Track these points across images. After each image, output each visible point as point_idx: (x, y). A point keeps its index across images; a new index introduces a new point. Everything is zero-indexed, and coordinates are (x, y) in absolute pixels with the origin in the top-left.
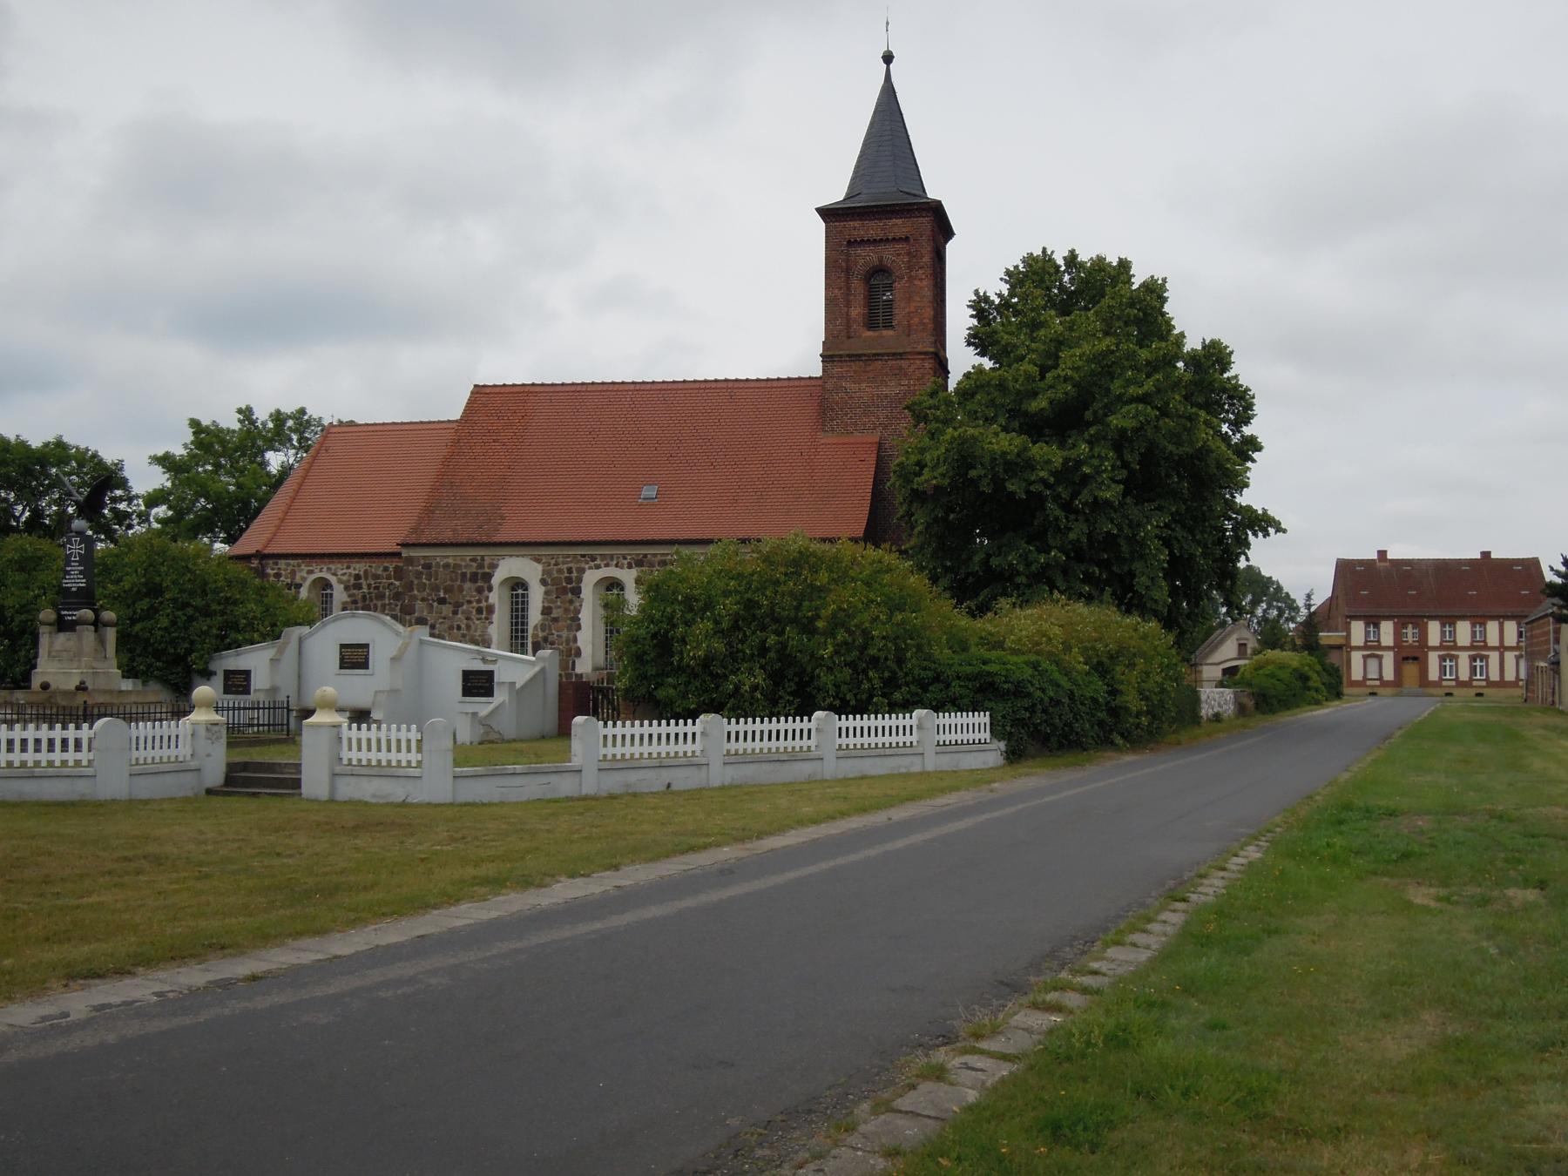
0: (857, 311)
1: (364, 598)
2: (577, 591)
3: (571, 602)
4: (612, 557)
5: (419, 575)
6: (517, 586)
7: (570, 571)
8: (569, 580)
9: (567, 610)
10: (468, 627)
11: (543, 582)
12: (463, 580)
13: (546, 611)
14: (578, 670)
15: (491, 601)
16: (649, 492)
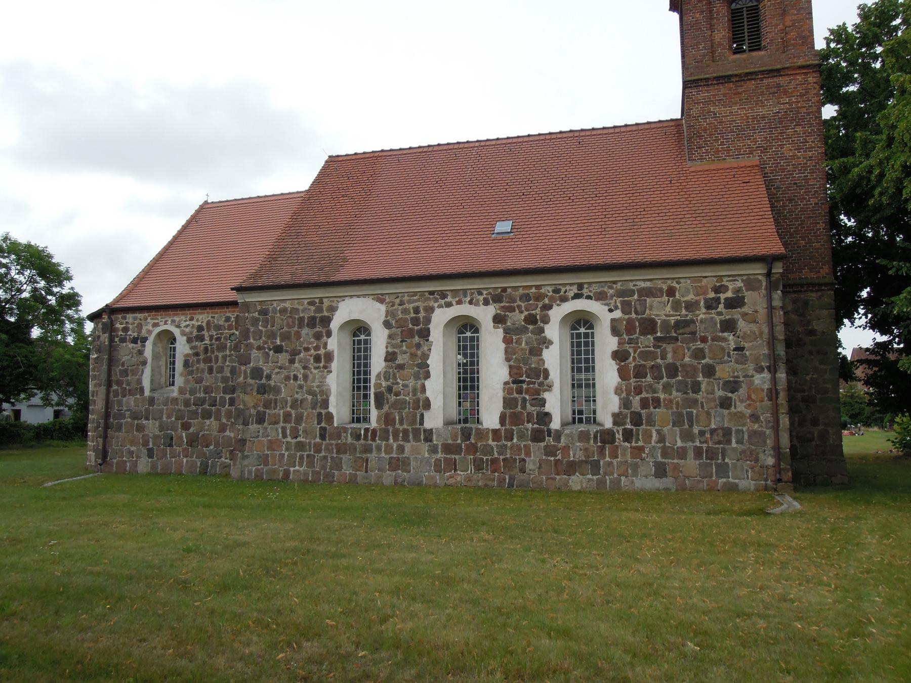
0: (722, 34)
1: (206, 350)
2: (425, 334)
3: (418, 346)
5: (255, 322)
6: (359, 329)
7: (417, 310)
8: (416, 321)
9: (413, 356)
10: (306, 377)
11: (387, 324)
12: (301, 326)
13: (390, 357)
14: (428, 425)
15: (329, 347)
16: (504, 227)
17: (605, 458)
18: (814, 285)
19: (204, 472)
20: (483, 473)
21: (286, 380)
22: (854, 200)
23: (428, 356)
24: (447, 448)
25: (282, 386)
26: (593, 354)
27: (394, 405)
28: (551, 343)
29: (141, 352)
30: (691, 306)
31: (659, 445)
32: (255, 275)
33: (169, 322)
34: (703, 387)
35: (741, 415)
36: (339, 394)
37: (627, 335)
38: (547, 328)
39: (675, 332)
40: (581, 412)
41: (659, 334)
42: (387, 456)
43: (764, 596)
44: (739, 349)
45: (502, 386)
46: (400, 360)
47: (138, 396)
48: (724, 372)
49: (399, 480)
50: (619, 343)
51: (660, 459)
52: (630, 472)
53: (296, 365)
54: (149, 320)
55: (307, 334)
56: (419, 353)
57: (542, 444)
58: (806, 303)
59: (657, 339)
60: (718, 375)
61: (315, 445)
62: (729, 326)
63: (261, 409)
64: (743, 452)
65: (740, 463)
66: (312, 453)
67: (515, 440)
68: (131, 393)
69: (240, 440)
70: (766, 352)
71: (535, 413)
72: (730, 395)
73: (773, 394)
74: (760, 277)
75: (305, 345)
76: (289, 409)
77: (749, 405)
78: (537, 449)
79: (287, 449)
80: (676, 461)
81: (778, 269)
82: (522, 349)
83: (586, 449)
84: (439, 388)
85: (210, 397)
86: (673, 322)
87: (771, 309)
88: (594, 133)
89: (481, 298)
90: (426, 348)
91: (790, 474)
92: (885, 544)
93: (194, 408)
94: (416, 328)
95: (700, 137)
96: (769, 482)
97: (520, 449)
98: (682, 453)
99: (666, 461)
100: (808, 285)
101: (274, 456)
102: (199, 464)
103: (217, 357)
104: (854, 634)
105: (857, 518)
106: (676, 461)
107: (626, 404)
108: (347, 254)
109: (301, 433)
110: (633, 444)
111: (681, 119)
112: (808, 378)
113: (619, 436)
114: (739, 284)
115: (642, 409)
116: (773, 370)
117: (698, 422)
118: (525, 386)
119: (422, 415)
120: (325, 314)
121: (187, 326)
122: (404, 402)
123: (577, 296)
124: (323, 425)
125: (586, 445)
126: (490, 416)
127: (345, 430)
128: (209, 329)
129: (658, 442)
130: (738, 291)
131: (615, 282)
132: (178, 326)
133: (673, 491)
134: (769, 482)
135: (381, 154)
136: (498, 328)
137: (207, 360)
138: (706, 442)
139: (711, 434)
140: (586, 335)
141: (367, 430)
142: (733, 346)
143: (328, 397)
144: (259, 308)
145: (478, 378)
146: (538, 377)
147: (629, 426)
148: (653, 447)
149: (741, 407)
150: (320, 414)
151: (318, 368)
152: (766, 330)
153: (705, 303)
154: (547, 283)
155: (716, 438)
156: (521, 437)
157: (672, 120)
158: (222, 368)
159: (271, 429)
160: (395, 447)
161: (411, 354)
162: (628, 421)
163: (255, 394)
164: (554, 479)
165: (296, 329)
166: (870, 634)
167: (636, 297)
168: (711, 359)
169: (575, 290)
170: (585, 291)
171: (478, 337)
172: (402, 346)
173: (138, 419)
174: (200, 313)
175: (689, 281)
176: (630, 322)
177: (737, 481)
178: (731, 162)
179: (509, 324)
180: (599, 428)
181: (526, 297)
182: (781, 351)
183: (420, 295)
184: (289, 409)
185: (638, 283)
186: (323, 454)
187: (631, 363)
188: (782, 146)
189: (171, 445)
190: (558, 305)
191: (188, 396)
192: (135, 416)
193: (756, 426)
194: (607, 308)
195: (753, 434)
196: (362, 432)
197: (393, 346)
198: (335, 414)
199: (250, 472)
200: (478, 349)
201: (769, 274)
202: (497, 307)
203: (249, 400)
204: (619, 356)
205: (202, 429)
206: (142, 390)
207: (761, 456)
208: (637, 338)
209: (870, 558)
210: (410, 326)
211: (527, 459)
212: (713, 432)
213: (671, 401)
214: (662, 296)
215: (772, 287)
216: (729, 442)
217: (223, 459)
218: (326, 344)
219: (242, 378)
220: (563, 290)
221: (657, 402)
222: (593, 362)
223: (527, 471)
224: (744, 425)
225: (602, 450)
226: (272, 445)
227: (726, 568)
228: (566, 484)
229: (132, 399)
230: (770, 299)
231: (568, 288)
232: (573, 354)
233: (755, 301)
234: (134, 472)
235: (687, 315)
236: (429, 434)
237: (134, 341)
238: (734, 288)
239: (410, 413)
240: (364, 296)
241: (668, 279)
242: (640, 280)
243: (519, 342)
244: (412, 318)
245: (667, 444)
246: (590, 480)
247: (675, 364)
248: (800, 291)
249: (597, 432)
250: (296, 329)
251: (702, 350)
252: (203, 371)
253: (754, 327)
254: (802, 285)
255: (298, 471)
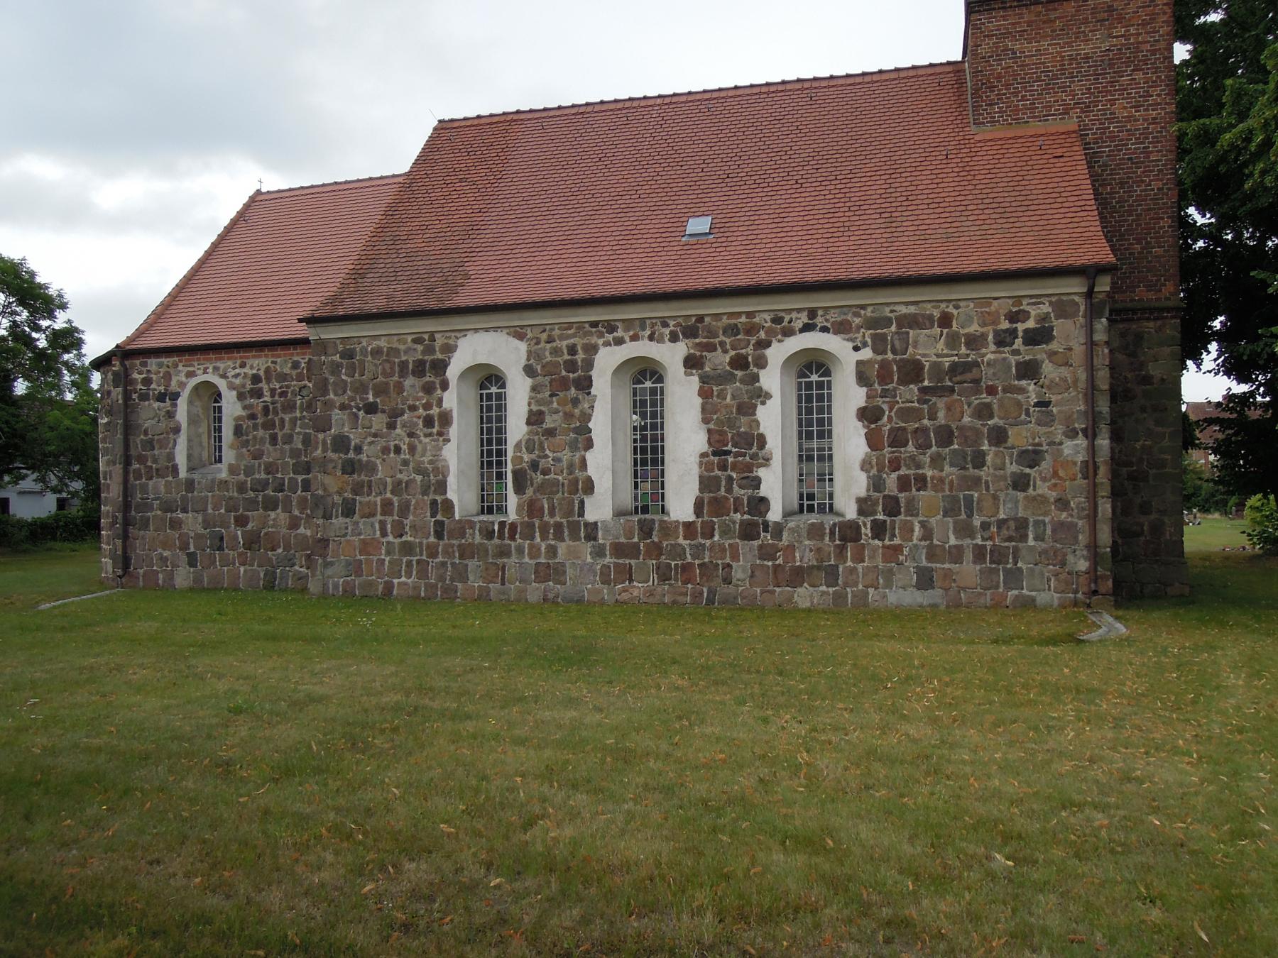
1: (266, 410)
2: (585, 384)
3: (575, 402)
4: (642, 322)
5: (336, 369)
6: (488, 379)
7: (572, 350)
8: (571, 366)
9: (568, 416)
10: (412, 449)
11: (529, 371)
13: (534, 419)
14: (590, 516)
15: (446, 405)
16: (699, 225)
17: (845, 562)
18: (1152, 310)
19: (270, 585)
20: (670, 585)
21: (383, 453)
22: (1212, 186)
23: (590, 416)
24: (619, 550)
25: (378, 462)
26: (830, 412)
27: (541, 488)
28: (768, 396)
29: (171, 415)
30: (974, 342)
31: (922, 543)
32: (333, 300)
33: (210, 370)
34: (989, 459)
35: (1043, 500)
36: (461, 473)
37: (880, 384)
38: (763, 374)
39: (950, 380)
40: (811, 497)
41: (926, 383)
42: (533, 562)
43: (1097, 772)
44: (1043, 404)
45: (698, 460)
46: (549, 422)
47: (170, 479)
48: (1019, 437)
49: (551, 596)
50: (868, 397)
51: (924, 563)
52: (881, 581)
53: (398, 431)
54: (180, 368)
55: (413, 386)
56: (577, 412)
57: (756, 543)
58: (1139, 337)
59: (924, 390)
60: (1010, 441)
61: (428, 546)
62: (1029, 370)
63: (348, 495)
64: (1045, 552)
65: (1038, 568)
66: (424, 557)
67: (716, 538)
68: (159, 473)
69: (320, 540)
70: (1082, 408)
71: (745, 498)
72: (1027, 470)
73: (1089, 468)
74: (1076, 298)
75: (410, 402)
76: (389, 495)
77: (1055, 485)
78: (748, 549)
79: (388, 553)
80: (947, 566)
81: (1104, 285)
82: (727, 406)
83: (819, 550)
84: (606, 461)
85: (275, 478)
86: (947, 364)
87: (1091, 344)
88: (832, 83)
89: (667, 331)
90: (586, 406)
91: (1110, 583)
92: (1256, 687)
93: (252, 494)
94: (571, 375)
95: (992, 88)
96: (1080, 595)
97: (723, 550)
98: (956, 555)
99: (933, 565)
100: (1144, 310)
101: (369, 562)
102: (262, 575)
103: (282, 421)
104: (1236, 835)
105: (1211, 648)
106: (947, 566)
107: (876, 484)
108: (469, 267)
109: (407, 529)
110: (887, 542)
111: (962, 62)
112: (1138, 445)
113: (866, 531)
114: (1046, 308)
115: (900, 491)
116: (1091, 433)
117: (980, 510)
118: (730, 459)
119: (582, 503)
120: (439, 356)
121: (236, 376)
122: (556, 483)
123: (807, 328)
124: (439, 517)
125: (819, 544)
126: (681, 503)
127: (472, 525)
128: (268, 380)
129: (923, 538)
130: (1044, 318)
131: (863, 307)
132: (224, 376)
133: (943, 607)
134: (1080, 595)
135: (515, 117)
136: (692, 374)
137: (269, 425)
138: (991, 538)
139: (999, 528)
140: (820, 385)
141: (502, 524)
142: (1033, 399)
143: (445, 477)
144: (340, 348)
145: (662, 447)
146: (750, 446)
147: (881, 517)
148: (916, 546)
149: (1043, 489)
150: (434, 502)
151: (430, 435)
152: (1083, 376)
153: (994, 337)
154: (763, 308)
155: (1005, 532)
156: (724, 533)
157: (949, 63)
158: (291, 436)
159: (365, 523)
160: (543, 549)
161: (565, 414)
162: (880, 508)
163: (339, 473)
164: (773, 592)
165: (396, 378)
166: (1261, 834)
167: (893, 328)
168: (1001, 418)
169: (804, 318)
170: (819, 321)
171: (662, 388)
172: (552, 402)
173: (172, 511)
174: (254, 357)
175: (972, 305)
176: (884, 365)
177: (1033, 593)
178: (1036, 127)
179: (707, 369)
180: (837, 519)
181: (732, 330)
182: (1104, 406)
183: (578, 328)
184: (389, 495)
185: (897, 308)
186: (440, 559)
187: (885, 425)
188: (1112, 102)
189: (220, 548)
190: (779, 341)
191: (242, 477)
192: (168, 507)
193: (1064, 515)
194: (851, 345)
195: (1059, 526)
196: (496, 528)
197: (539, 402)
198: (456, 502)
199: (336, 586)
200: (662, 406)
201: (1090, 294)
202: (690, 344)
203: (332, 483)
204: (868, 415)
205: (265, 525)
206: (175, 469)
207: (1070, 558)
208: (895, 389)
209: (1238, 708)
210: (564, 373)
211: (734, 564)
212: (1001, 524)
213: (942, 480)
214: (932, 326)
215: (1093, 312)
216: (1024, 538)
217: (297, 568)
218: (440, 401)
219: (319, 451)
220: (787, 318)
221: (922, 482)
222: (830, 424)
223: (734, 581)
224: (1045, 514)
225: (841, 550)
226: (366, 547)
227: (1036, 729)
228: (790, 599)
229: (161, 483)
230: (1090, 331)
231: (794, 315)
232: (800, 413)
233: (1069, 334)
234: (170, 586)
235: (968, 355)
236: (592, 530)
237: (161, 398)
238: (1039, 315)
239: (564, 499)
240: (496, 329)
241: (941, 301)
242: (900, 302)
243: (722, 395)
244: (565, 362)
245: (935, 542)
246: (823, 593)
247: (948, 426)
248: (1132, 320)
249: (835, 525)
250: (396, 378)
251: (988, 406)
252: (262, 440)
253: (1065, 372)
254: (1134, 311)
255: (406, 584)
